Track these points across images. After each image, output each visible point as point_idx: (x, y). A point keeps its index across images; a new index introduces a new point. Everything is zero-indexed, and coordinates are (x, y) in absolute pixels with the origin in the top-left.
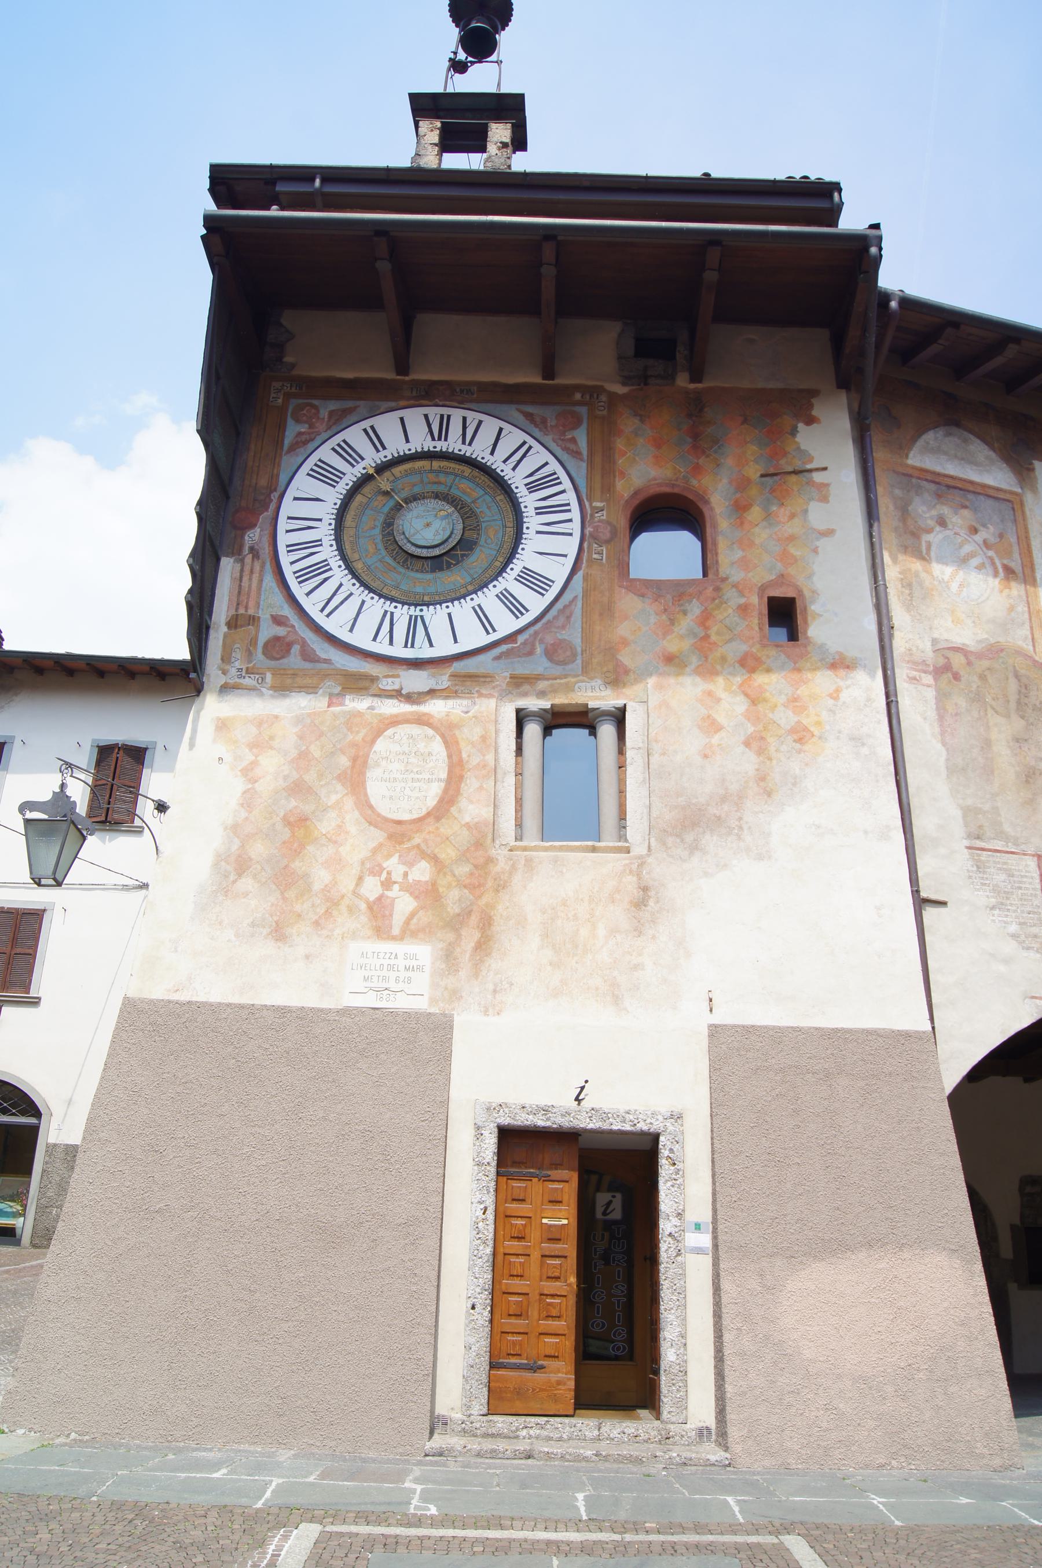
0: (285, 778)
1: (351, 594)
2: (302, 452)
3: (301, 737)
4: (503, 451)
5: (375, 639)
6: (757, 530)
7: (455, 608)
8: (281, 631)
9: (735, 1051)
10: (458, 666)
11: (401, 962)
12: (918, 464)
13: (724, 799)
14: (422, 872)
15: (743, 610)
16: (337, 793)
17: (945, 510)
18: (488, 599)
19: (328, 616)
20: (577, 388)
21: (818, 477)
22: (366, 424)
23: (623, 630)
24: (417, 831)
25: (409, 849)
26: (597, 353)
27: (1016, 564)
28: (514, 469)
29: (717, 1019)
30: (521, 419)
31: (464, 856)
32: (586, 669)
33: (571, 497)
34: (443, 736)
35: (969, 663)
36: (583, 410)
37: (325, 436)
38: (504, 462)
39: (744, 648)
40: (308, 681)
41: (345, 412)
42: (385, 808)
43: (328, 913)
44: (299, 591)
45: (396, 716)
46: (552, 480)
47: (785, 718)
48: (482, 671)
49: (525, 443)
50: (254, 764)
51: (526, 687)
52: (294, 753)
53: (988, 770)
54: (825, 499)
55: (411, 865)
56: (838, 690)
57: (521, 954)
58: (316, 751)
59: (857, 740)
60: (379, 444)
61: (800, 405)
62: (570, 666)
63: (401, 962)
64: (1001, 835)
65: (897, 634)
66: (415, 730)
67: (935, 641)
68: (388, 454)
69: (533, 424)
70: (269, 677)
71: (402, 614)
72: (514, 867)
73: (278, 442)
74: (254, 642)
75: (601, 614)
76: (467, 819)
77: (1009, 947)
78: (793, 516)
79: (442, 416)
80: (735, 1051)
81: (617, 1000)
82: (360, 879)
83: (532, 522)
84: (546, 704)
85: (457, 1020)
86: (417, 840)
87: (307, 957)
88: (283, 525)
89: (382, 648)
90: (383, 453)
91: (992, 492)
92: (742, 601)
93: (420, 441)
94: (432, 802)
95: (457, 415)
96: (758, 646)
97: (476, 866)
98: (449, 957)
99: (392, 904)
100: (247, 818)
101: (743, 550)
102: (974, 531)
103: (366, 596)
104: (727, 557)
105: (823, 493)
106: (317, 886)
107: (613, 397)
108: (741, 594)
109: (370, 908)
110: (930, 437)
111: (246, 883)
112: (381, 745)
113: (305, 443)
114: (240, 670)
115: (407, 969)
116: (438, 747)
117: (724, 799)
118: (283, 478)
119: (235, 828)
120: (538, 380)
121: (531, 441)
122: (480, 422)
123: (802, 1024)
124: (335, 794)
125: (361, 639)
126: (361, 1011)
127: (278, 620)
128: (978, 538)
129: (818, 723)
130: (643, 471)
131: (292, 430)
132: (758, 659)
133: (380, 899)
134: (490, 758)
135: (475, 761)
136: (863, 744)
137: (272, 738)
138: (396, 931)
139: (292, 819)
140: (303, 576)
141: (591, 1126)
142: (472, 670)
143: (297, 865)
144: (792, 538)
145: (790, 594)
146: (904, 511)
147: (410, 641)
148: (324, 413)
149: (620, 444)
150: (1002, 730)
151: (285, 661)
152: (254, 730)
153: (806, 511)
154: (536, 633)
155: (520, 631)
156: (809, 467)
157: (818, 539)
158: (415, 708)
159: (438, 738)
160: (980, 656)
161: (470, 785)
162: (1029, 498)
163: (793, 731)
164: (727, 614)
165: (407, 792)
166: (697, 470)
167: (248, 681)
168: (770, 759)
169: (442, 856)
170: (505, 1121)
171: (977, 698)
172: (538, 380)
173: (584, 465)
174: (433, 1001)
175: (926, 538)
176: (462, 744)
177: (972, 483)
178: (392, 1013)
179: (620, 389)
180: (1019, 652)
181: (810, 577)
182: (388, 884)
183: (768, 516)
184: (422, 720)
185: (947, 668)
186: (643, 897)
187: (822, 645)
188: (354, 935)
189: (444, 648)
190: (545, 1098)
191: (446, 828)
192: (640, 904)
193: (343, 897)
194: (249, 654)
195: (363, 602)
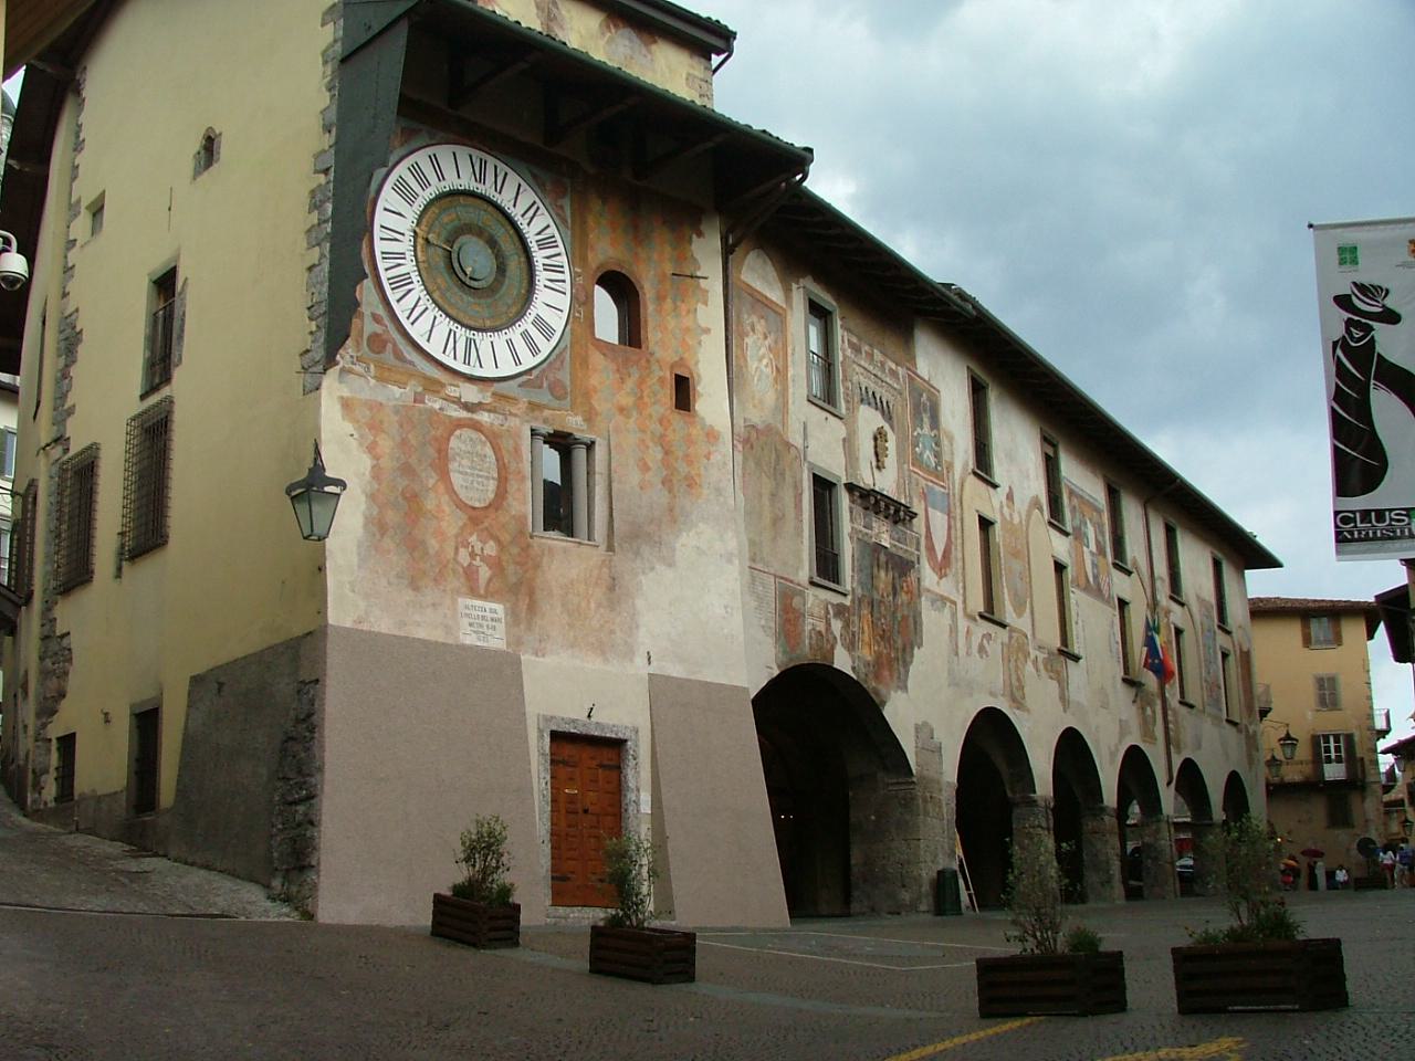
0: (398, 459)
1: (427, 309)
3: (401, 426)
5: (444, 352)
6: (669, 318)
8: (378, 329)
9: (660, 688)
10: (497, 386)
11: (488, 614)
12: (746, 280)
14: (491, 549)
16: (432, 477)
17: (754, 319)
19: (412, 324)
22: (430, 151)
23: (594, 381)
24: (487, 517)
25: (482, 530)
28: (529, 224)
33: (563, 260)
34: (491, 443)
35: (758, 438)
37: (402, 151)
38: (523, 215)
39: (662, 410)
40: (398, 377)
42: (463, 494)
44: (392, 297)
45: (459, 419)
48: (511, 394)
49: (535, 202)
51: (537, 413)
52: (398, 439)
54: (706, 303)
55: (485, 543)
56: (709, 453)
57: (553, 614)
62: (563, 402)
66: (474, 435)
67: (745, 420)
68: (446, 186)
70: (372, 366)
71: (462, 333)
75: (581, 364)
76: (514, 513)
78: (689, 312)
79: (481, 160)
80: (660, 688)
81: (603, 653)
82: (457, 549)
83: (542, 277)
85: (522, 658)
86: (486, 524)
87: (434, 605)
89: (448, 360)
90: (443, 183)
91: (774, 307)
92: (662, 374)
93: (467, 182)
94: (491, 496)
95: (491, 161)
96: (669, 412)
97: (522, 549)
98: (514, 617)
99: (478, 571)
100: (378, 490)
101: (662, 332)
102: (766, 338)
104: (652, 334)
105: (704, 297)
106: (431, 552)
108: (661, 367)
109: (465, 572)
111: (388, 543)
112: (454, 443)
114: (352, 357)
115: (492, 620)
116: (488, 451)
117: (651, 522)
121: (539, 203)
122: (506, 174)
123: (693, 677)
125: (434, 349)
128: (767, 343)
129: (699, 475)
132: (669, 421)
133: (470, 564)
135: (513, 466)
136: (721, 494)
137: (381, 422)
138: (482, 592)
139: (408, 495)
141: (596, 734)
142: (505, 393)
144: (687, 330)
147: (467, 361)
150: (767, 485)
151: (382, 355)
152: (368, 413)
153: (696, 310)
154: (544, 370)
155: (534, 368)
156: (699, 274)
157: (701, 334)
158: (469, 415)
159: (488, 444)
161: (513, 486)
162: (789, 312)
163: (686, 478)
164: (653, 381)
165: (475, 485)
167: (358, 368)
168: (675, 497)
169: (502, 539)
170: (554, 728)
171: (758, 464)
173: (569, 233)
174: (508, 645)
176: (504, 452)
177: (766, 297)
179: (592, 171)
180: (778, 433)
181: (697, 363)
182: (473, 555)
183: (676, 308)
184: (476, 426)
186: (613, 585)
187: (703, 419)
188: (457, 592)
189: (488, 371)
190: (571, 712)
192: (612, 588)
193: (448, 561)
195: (435, 318)
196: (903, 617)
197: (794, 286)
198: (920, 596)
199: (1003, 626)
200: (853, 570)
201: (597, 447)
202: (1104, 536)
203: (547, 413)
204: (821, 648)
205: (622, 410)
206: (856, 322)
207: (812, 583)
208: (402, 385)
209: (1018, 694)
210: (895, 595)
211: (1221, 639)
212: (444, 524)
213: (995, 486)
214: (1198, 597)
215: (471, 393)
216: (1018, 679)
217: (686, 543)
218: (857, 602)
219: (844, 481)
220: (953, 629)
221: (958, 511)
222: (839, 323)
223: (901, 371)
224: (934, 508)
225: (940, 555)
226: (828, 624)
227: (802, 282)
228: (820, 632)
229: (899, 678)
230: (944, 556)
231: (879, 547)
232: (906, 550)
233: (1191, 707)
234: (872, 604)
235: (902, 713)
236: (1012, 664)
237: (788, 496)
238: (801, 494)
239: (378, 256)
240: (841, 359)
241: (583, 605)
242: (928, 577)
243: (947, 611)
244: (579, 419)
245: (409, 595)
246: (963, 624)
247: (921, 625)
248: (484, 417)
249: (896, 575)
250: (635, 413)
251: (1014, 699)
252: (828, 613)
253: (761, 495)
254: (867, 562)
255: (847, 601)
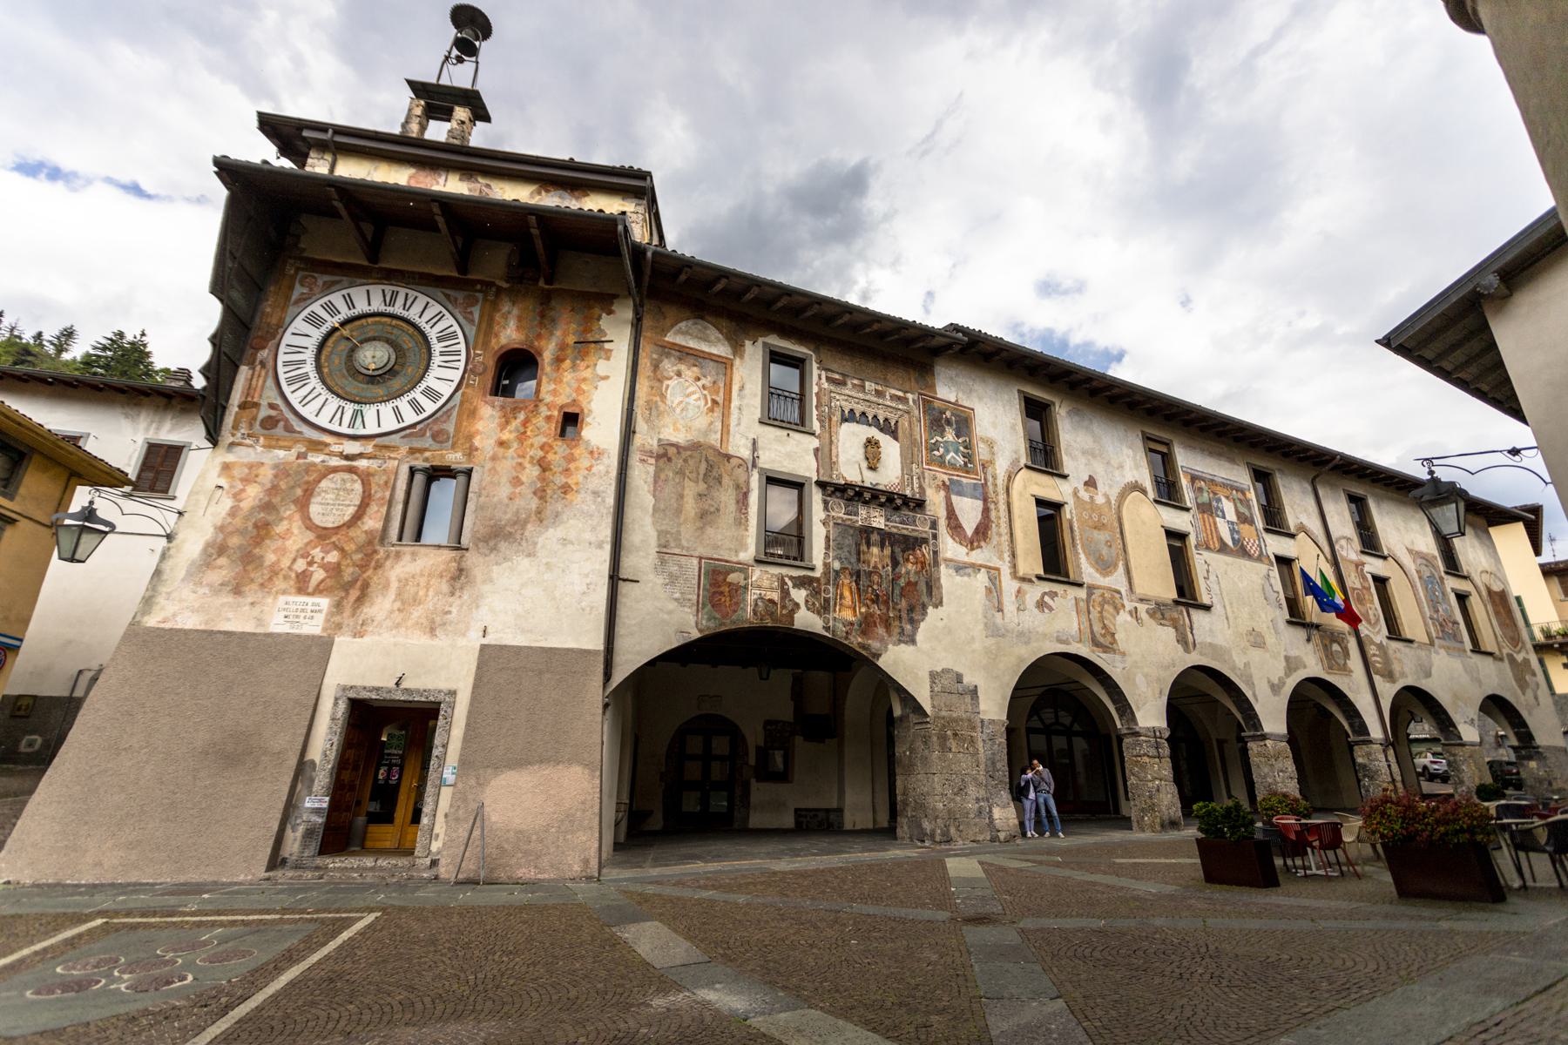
2: (303, 304)
3: (276, 476)
4: (427, 316)
7: (382, 407)
8: (273, 413)
9: (492, 659)
10: (378, 441)
13: (515, 523)
15: (548, 418)
17: (683, 367)
18: (403, 403)
20: (479, 281)
21: (607, 346)
22: (345, 292)
23: (480, 426)
26: (495, 262)
27: (720, 399)
29: (485, 641)
30: (441, 297)
31: (359, 549)
32: (453, 447)
33: (462, 347)
36: (480, 296)
41: (334, 283)
42: (318, 520)
43: (270, 579)
46: (453, 336)
47: (560, 480)
50: (243, 490)
52: (269, 486)
53: (679, 511)
54: (608, 359)
57: (381, 606)
58: (283, 485)
59: (596, 493)
60: (350, 304)
61: (606, 301)
63: (309, 608)
64: (679, 546)
65: (637, 436)
66: (346, 476)
69: (449, 303)
71: (350, 408)
72: (388, 557)
73: (288, 298)
74: (254, 418)
76: (366, 528)
77: (672, 606)
80: (492, 659)
81: (432, 631)
82: (294, 560)
83: (437, 359)
84: (427, 465)
85: (337, 639)
86: (334, 539)
88: (282, 349)
89: (335, 427)
93: (377, 305)
94: (347, 518)
95: (402, 292)
98: (338, 606)
103: (330, 396)
106: (267, 563)
107: (499, 290)
109: (298, 576)
110: (683, 325)
111: (223, 561)
112: (324, 484)
113: (305, 300)
116: (358, 486)
117: (515, 523)
118: (288, 320)
119: (221, 529)
120: (456, 274)
124: (290, 511)
125: (322, 421)
126: (279, 635)
127: (272, 406)
130: (510, 334)
131: (299, 290)
134: (388, 494)
140: (290, 382)
143: (257, 551)
144: (584, 380)
145: (576, 411)
146: (656, 367)
148: (320, 282)
149: (498, 317)
150: (691, 490)
160: (685, 449)
161: (373, 508)
162: (737, 362)
164: (539, 421)
166: (539, 336)
167: (248, 441)
170: (352, 695)
172: (456, 274)
174: (324, 629)
175: (666, 382)
178: (299, 636)
179: (505, 285)
180: (712, 447)
184: (351, 470)
185: (665, 455)
188: (284, 592)
189: (372, 429)
191: (353, 533)
194: (251, 426)
196: (909, 583)
197: (748, 343)
198: (936, 563)
199: (1081, 585)
200: (827, 548)
201: (474, 475)
202: (1249, 507)
203: (427, 454)
204: (772, 614)
205: (502, 443)
206: (841, 365)
207: (758, 562)
208: (288, 448)
209: (1105, 641)
210: (895, 563)
211: (1451, 583)
212: (289, 543)
213: (1065, 477)
214: (1410, 551)
215: (352, 448)
216: (1105, 627)
217: (548, 539)
218: (832, 575)
219: (815, 478)
220: (994, 589)
221: (1002, 498)
222: (815, 366)
223: (910, 396)
224: (960, 494)
225: (969, 532)
226: (785, 594)
227: (761, 340)
228: (771, 601)
229: (902, 632)
230: (977, 531)
231: (866, 532)
232: (923, 529)
233: (1411, 641)
234: (857, 575)
235: (909, 662)
236: (1095, 614)
237: (727, 497)
238: (746, 495)
239: (280, 364)
240: (815, 389)
241: (421, 593)
242: (950, 548)
243: (982, 578)
244: (459, 455)
245: (228, 599)
246: (1009, 585)
247: (940, 587)
248: (362, 464)
249: (897, 550)
250: (515, 445)
251: (1096, 643)
252: (783, 583)
253: (682, 496)
254: (849, 541)
255: (817, 574)
